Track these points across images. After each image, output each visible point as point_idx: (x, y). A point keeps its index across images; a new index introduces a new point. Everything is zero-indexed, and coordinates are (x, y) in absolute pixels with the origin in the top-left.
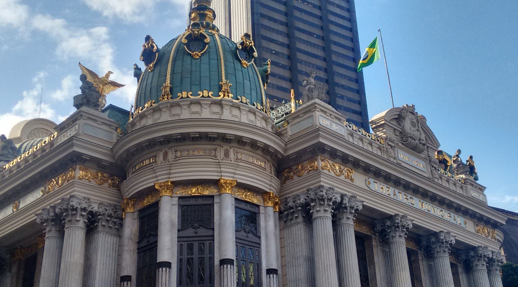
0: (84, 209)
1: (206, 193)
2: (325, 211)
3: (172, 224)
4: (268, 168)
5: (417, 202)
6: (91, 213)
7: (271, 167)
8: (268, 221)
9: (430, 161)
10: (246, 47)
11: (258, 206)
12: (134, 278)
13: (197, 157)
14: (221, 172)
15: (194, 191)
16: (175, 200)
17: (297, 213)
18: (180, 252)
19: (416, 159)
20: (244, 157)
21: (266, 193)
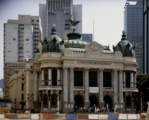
7: (59, 62)
9: (101, 52)
16: (44, 70)
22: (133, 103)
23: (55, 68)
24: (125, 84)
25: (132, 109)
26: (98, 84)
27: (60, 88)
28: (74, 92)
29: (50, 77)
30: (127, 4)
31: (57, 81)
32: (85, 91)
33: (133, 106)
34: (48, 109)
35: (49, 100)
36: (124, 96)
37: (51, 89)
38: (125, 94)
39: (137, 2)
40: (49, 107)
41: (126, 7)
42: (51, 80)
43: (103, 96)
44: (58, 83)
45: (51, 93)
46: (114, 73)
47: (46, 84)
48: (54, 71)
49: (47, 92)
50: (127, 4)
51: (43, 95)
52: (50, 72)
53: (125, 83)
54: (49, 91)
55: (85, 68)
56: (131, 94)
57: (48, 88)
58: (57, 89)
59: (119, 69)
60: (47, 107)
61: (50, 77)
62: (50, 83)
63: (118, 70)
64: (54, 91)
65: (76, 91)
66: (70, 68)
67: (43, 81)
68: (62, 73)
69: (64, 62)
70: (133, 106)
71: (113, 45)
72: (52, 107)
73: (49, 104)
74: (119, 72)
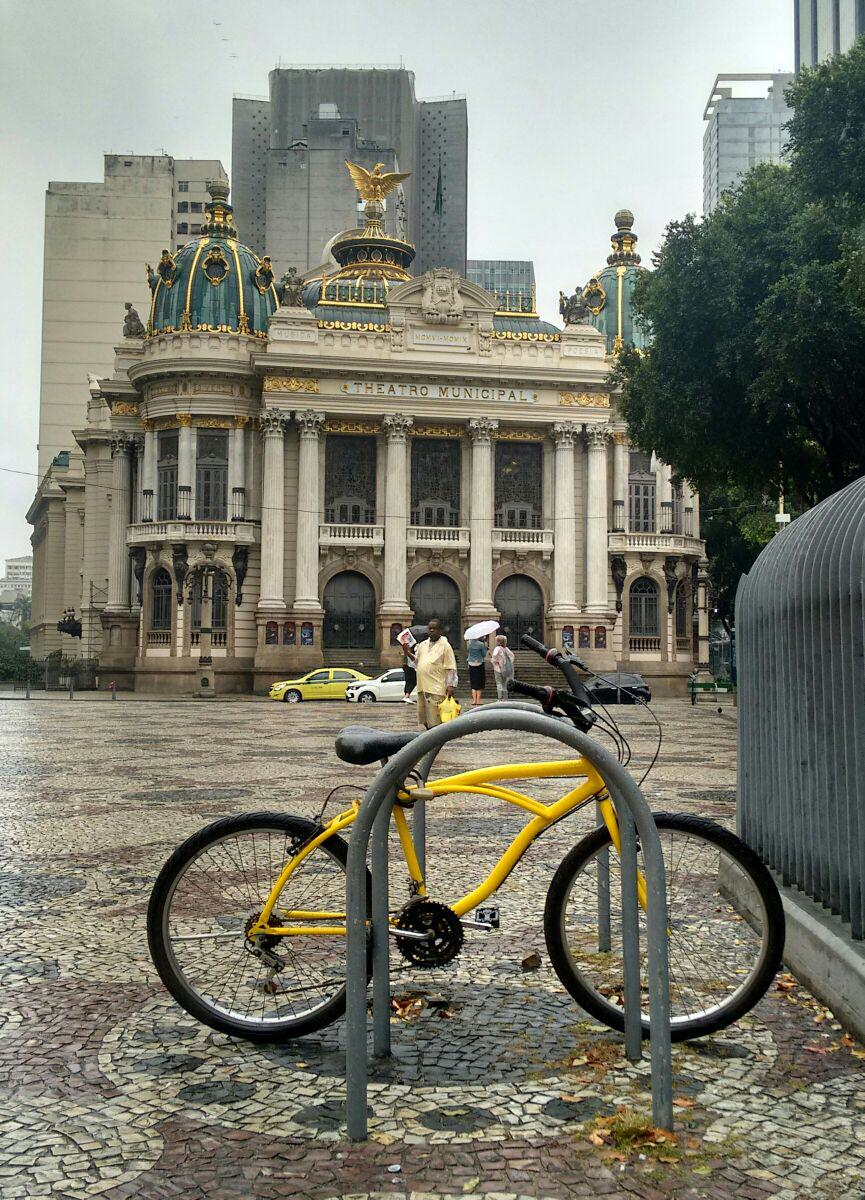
0: (121, 441)
1: (174, 426)
2: (271, 432)
3: (153, 456)
4: (237, 392)
5: (433, 392)
9: (478, 330)
10: (216, 263)
11: (228, 429)
13: (162, 394)
14: (177, 407)
15: (165, 426)
18: (160, 481)
19: (456, 335)
20: (203, 388)
21: (233, 416)
22: (670, 622)
24: (622, 513)
25: (665, 652)
26: (464, 511)
27: (244, 536)
28: (321, 557)
29: (187, 475)
30: (717, 98)
31: (230, 491)
33: (670, 639)
34: (173, 654)
36: (618, 582)
37: (190, 537)
38: (624, 567)
39: (770, 83)
40: (180, 642)
42: (194, 487)
43: (494, 581)
44: (234, 506)
45: (191, 562)
46: (555, 446)
47: (169, 513)
49: (167, 559)
50: (717, 98)
51: (147, 574)
52: (188, 444)
53: (622, 503)
54: (181, 550)
55: (388, 421)
56: (658, 570)
57: (175, 534)
58: (223, 538)
59: (584, 426)
61: (187, 475)
62: (187, 505)
63: (579, 429)
65: (332, 549)
66: (299, 417)
67: (149, 492)
69: (268, 384)
70: (670, 639)
71: (561, 293)
73: (180, 624)
74: (583, 442)
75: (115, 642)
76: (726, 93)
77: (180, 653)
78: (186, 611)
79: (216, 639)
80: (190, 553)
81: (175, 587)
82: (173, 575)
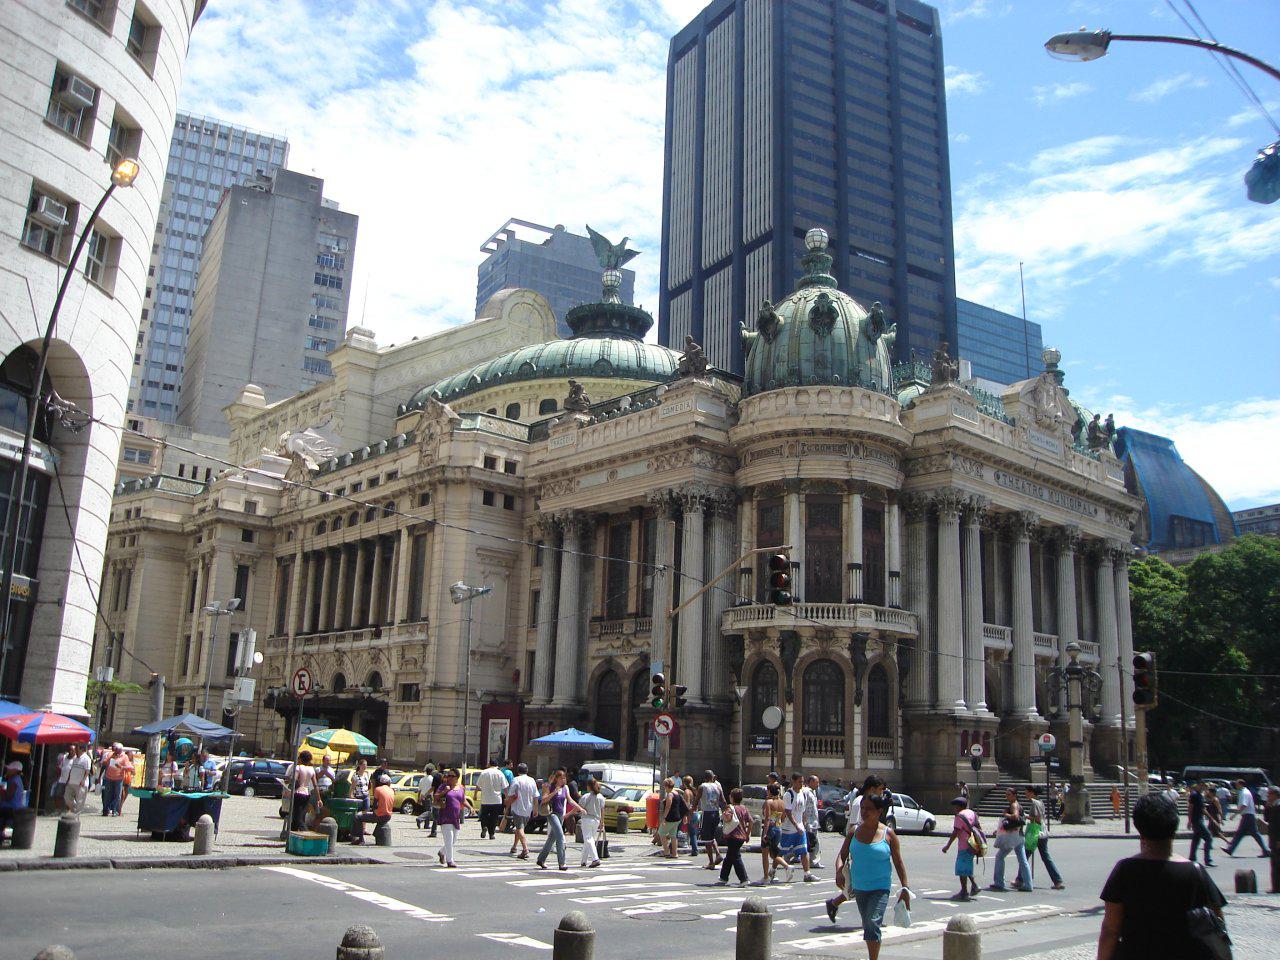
0: (702, 497)
6: (708, 499)
8: (893, 520)
12: (755, 571)
16: (803, 497)
17: (923, 514)
23: (829, 484)
32: (1011, 654)
34: (849, 765)
35: (858, 702)
40: (857, 751)
41: (493, 246)
44: (893, 590)
45: (869, 655)
48: (875, 502)
50: (503, 237)
60: (841, 748)
62: (855, 584)
64: (826, 635)
66: (974, 503)
68: (647, 525)
72: (871, 749)
73: (858, 729)
75: (696, 745)
76: (511, 234)
77: (857, 765)
78: (863, 714)
79: (871, 747)
80: (869, 644)
81: (850, 684)
82: (848, 669)
